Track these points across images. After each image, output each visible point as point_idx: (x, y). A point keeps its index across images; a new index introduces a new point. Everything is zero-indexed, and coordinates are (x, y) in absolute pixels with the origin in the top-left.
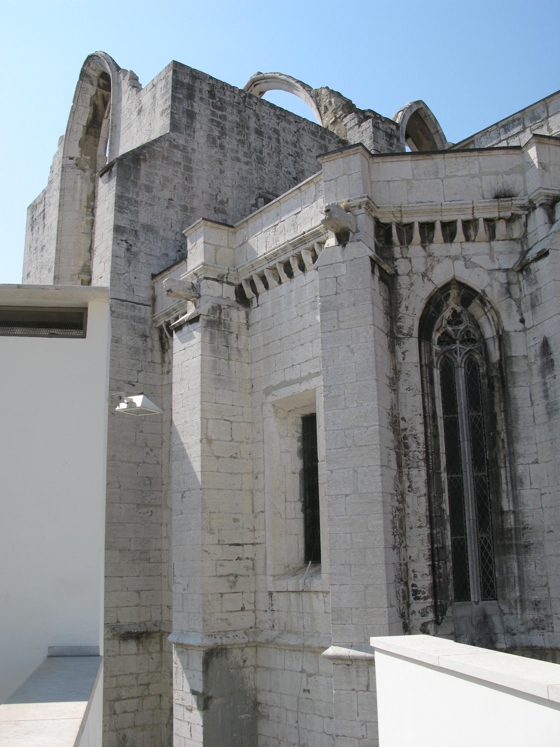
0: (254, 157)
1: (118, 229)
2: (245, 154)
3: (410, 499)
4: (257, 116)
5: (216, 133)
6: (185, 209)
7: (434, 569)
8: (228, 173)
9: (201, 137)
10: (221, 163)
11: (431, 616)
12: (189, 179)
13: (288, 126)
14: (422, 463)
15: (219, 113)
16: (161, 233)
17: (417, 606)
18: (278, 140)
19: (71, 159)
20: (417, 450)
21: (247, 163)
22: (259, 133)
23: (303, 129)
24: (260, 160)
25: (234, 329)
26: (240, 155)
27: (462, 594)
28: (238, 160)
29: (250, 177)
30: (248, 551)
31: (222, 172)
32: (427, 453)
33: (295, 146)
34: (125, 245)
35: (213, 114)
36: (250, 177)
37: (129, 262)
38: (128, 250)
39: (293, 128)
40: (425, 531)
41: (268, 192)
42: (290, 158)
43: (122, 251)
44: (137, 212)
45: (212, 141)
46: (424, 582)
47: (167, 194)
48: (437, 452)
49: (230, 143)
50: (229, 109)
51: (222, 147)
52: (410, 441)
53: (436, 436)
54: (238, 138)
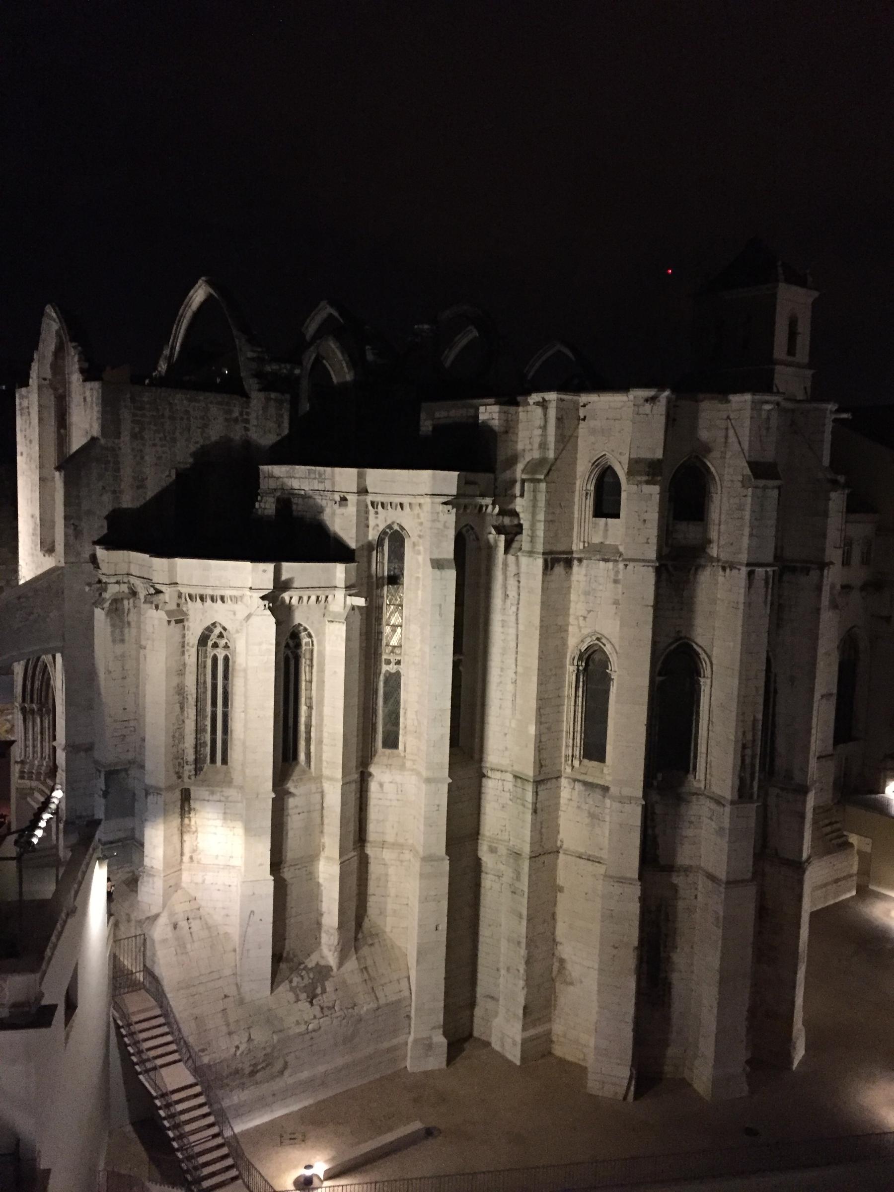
0: (168, 438)
1: (66, 518)
2: (161, 439)
3: (187, 721)
4: (170, 404)
5: (137, 430)
6: (114, 492)
7: (196, 752)
8: (147, 458)
9: (126, 437)
10: (141, 451)
11: (193, 772)
12: (118, 470)
13: (197, 405)
14: (195, 708)
15: (139, 412)
16: (98, 512)
17: (187, 767)
18: (188, 419)
19: (45, 379)
20: (192, 700)
21: (162, 446)
22: (172, 418)
23: (211, 403)
24: (174, 440)
25: (126, 611)
26: (157, 441)
27: (213, 760)
28: (154, 445)
29: (164, 456)
30: (132, 724)
31: (142, 458)
32: (197, 702)
33: (203, 419)
34: (72, 527)
35: (134, 415)
36: (164, 456)
37: (76, 537)
38: (75, 529)
39: (203, 404)
40: (194, 736)
41: (179, 463)
42: (199, 430)
43: (71, 531)
44: (79, 505)
45: (134, 436)
46: (191, 757)
47: (101, 484)
48: (205, 700)
49: (147, 435)
50: (147, 406)
51: (142, 438)
52: (189, 697)
53: (205, 692)
54: (155, 428)
